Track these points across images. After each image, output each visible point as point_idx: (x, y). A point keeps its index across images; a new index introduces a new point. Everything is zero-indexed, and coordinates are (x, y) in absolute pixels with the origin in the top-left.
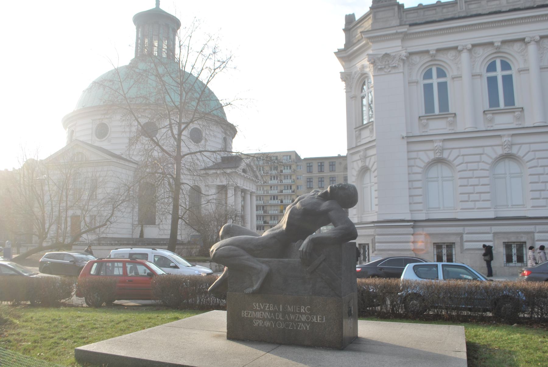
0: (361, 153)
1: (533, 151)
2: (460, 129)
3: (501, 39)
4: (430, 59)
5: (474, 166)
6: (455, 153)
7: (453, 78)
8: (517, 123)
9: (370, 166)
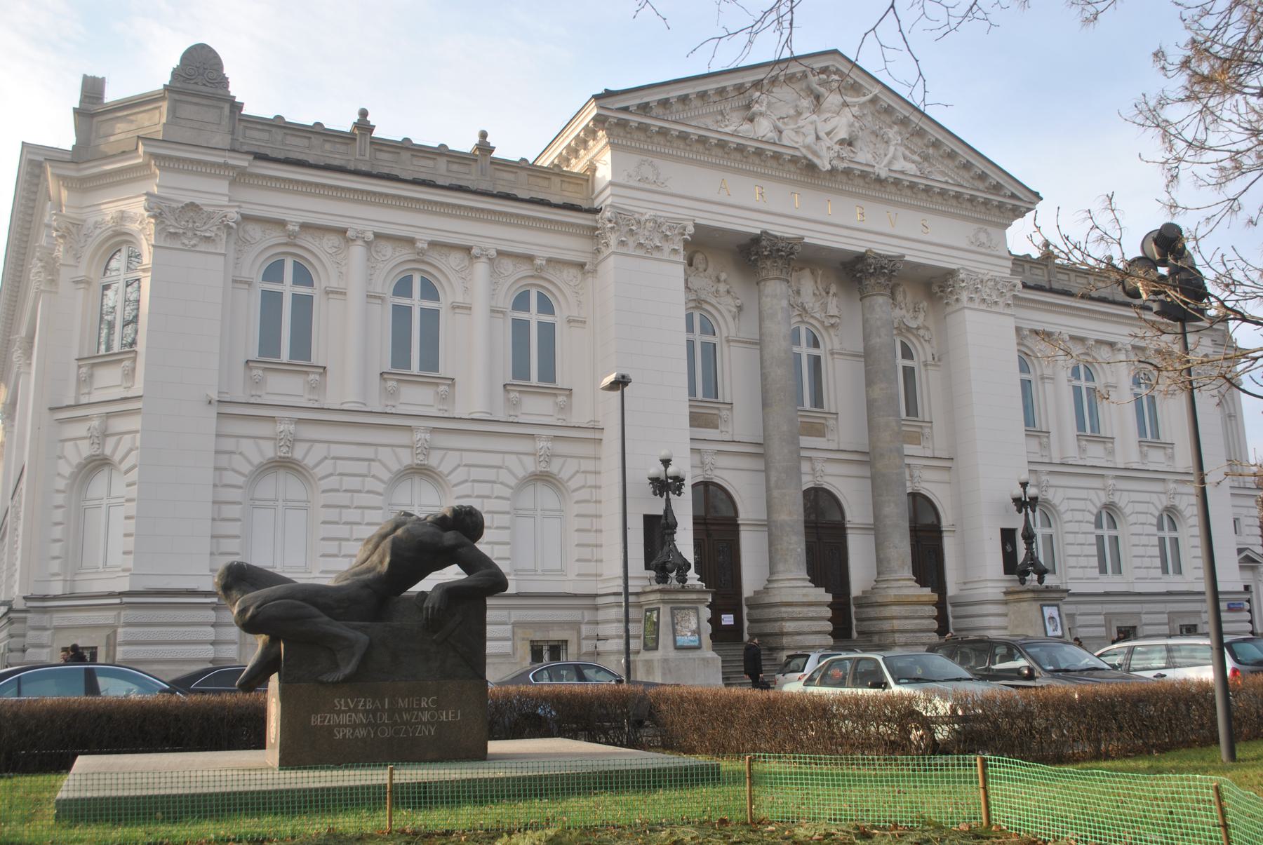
0: (95, 423)
1: (465, 465)
2: (331, 401)
3: (430, 239)
4: (284, 240)
6: (319, 451)
7: (327, 293)
8: (441, 407)
9: (117, 458)
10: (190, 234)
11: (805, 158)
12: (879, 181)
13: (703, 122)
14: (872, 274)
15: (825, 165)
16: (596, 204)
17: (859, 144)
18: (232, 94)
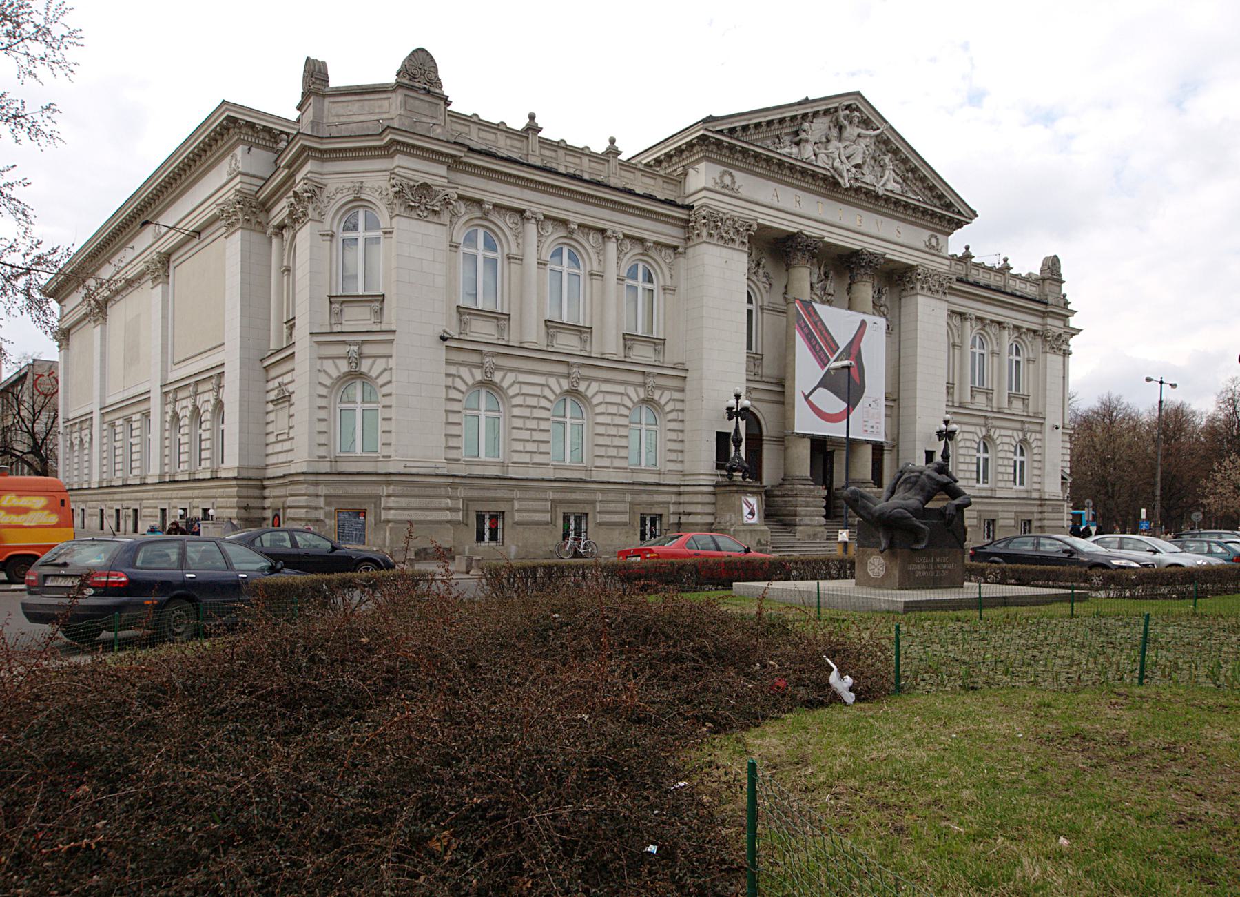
4: (479, 214)
5: (532, 401)
10: (423, 208)
11: (833, 177)
12: (877, 197)
13: (761, 144)
14: (863, 267)
15: (845, 182)
16: (687, 202)
17: (865, 170)
18: (445, 94)
